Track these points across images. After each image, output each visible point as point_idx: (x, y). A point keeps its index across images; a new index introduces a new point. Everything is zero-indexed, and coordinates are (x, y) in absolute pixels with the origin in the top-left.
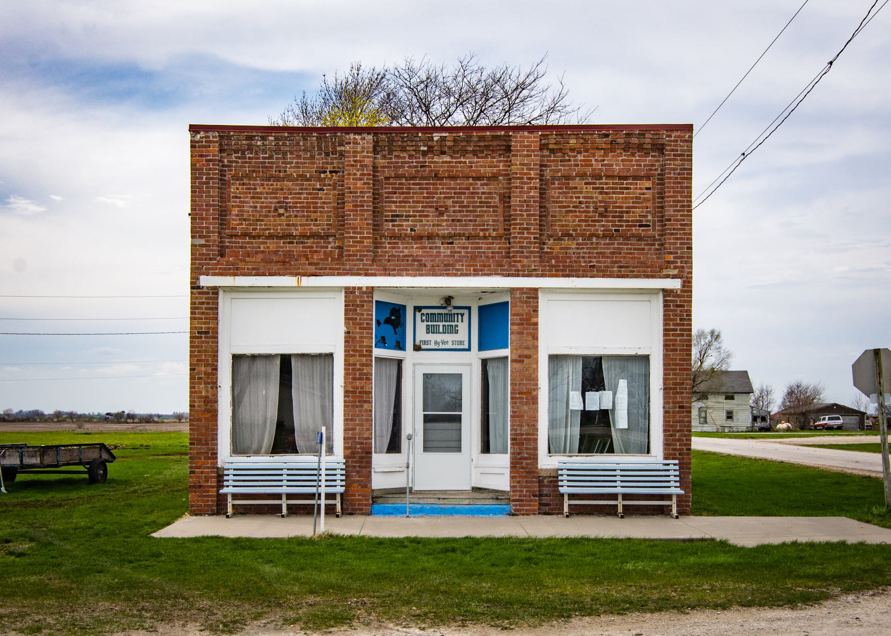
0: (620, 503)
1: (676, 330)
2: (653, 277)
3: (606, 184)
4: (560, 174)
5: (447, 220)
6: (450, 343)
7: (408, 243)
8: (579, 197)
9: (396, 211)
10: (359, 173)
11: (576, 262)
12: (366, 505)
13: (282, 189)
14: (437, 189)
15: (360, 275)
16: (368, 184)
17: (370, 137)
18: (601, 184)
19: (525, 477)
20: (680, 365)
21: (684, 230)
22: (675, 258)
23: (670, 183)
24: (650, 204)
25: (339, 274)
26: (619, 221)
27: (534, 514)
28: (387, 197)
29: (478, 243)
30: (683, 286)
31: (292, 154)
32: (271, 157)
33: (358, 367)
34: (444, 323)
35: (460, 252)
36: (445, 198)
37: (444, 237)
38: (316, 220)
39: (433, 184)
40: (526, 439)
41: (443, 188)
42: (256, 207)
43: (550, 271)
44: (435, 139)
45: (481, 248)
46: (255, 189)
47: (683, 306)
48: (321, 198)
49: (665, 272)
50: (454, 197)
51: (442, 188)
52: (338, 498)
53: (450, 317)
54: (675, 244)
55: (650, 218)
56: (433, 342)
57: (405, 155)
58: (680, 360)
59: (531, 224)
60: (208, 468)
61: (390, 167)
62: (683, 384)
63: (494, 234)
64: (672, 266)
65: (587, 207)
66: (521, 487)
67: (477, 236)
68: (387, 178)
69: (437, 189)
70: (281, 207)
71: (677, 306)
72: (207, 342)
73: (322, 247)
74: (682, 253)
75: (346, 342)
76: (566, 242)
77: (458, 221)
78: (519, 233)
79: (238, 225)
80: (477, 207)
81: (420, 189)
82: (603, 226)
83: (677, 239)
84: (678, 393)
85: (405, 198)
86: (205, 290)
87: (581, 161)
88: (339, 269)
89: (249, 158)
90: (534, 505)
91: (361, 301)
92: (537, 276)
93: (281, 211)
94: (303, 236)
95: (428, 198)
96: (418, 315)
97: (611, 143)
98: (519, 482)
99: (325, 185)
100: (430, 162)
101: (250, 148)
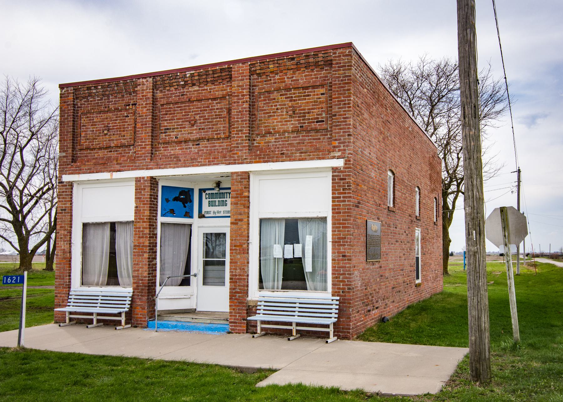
0: (294, 328)
1: (340, 197)
2: (323, 158)
3: (294, 94)
4: (264, 91)
5: (196, 129)
6: (222, 212)
7: (174, 147)
8: (277, 105)
9: (167, 126)
10: (144, 103)
11: (272, 151)
12: (144, 321)
13: (107, 118)
14: (190, 109)
15: (143, 169)
16: (149, 110)
17: (151, 79)
18: (291, 94)
19: (238, 306)
20: (343, 224)
21: (346, 121)
22: (339, 143)
23: (336, 88)
24: (324, 105)
25: (133, 170)
26: (303, 120)
27: (243, 333)
28: (162, 118)
29: (214, 143)
30: (345, 164)
31: (112, 96)
32: (101, 99)
33: (141, 229)
34: (219, 199)
35: (203, 150)
36: (195, 114)
37: (194, 141)
38: (124, 136)
39: (189, 106)
40: (238, 279)
41: (194, 108)
42: (93, 131)
43: (255, 159)
44: (188, 76)
45: (216, 146)
46: (93, 120)
47: (345, 179)
48: (127, 122)
49: (332, 154)
50: (200, 114)
51: (194, 108)
52: (123, 315)
53: (222, 195)
54: (339, 133)
55: (324, 115)
56: (212, 212)
57: (172, 89)
58: (343, 220)
59: (244, 127)
60: (64, 294)
61: (164, 98)
62: (345, 238)
63: (223, 136)
64: (337, 149)
65: (282, 112)
66: (235, 313)
67: (213, 139)
68: (162, 105)
69: (190, 109)
70: (105, 130)
71: (341, 179)
72: (65, 216)
73: (127, 153)
74: (344, 139)
75: (136, 213)
76: (268, 138)
77: (203, 129)
78: (236, 134)
79: (84, 142)
80: (214, 118)
81: (181, 110)
82: (292, 124)
83: (341, 129)
84: (341, 245)
85: (172, 117)
86: (65, 184)
87: (278, 79)
88: (132, 166)
89: (91, 101)
90: (243, 327)
91: (144, 186)
92: (247, 163)
93: (106, 132)
94: (117, 147)
95: (185, 115)
96: (204, 194)
97: (297, 64)
98: (234, 309)
99: (129, 114)
100: (187, 92)
101: (90, 95)
